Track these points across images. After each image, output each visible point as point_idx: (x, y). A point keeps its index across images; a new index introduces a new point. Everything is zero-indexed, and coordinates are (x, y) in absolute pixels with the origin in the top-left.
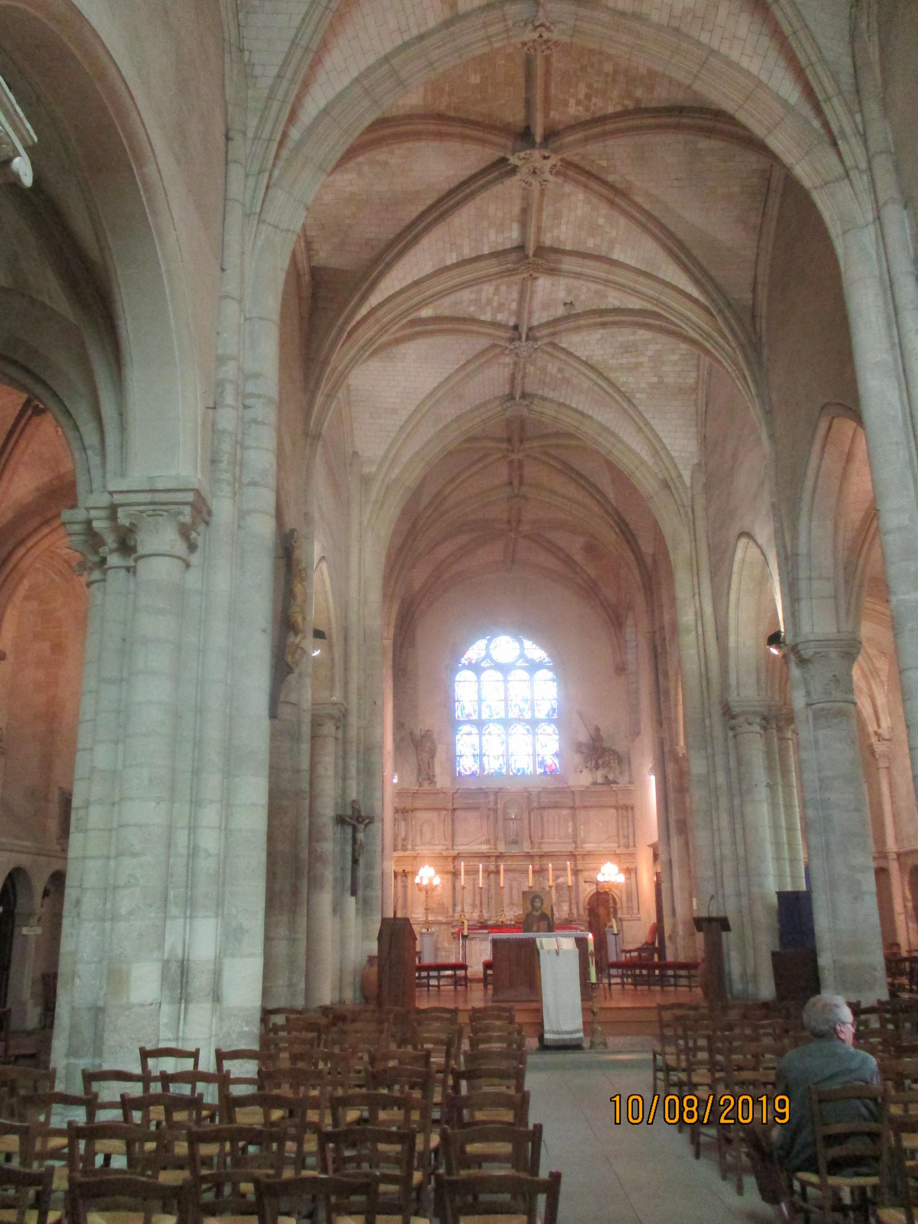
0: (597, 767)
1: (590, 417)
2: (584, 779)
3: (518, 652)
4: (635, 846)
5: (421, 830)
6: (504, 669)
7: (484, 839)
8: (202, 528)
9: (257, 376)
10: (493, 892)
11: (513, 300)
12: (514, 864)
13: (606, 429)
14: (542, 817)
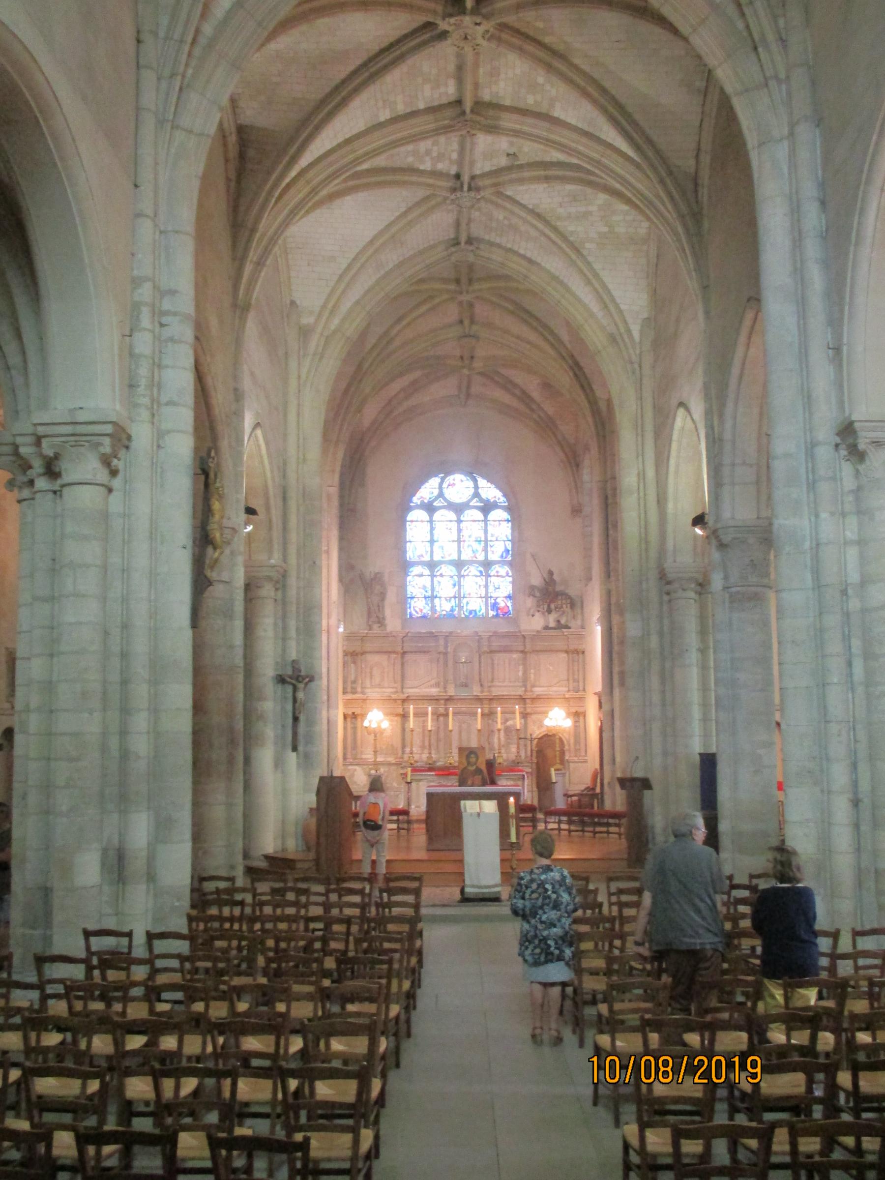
0: (549, 611)
1: (538, 265)
2: (537, 623)
3: (472, 490)
4: (584, 690)
5: (371, 673)
6: (459, 509)
7: (433, 682)
8: (122, 453)
9: (173, 292)
10: (442, 734)
11: (453, 151)
12: (463, 707)
13: (555, 278)
14: (493, 660)
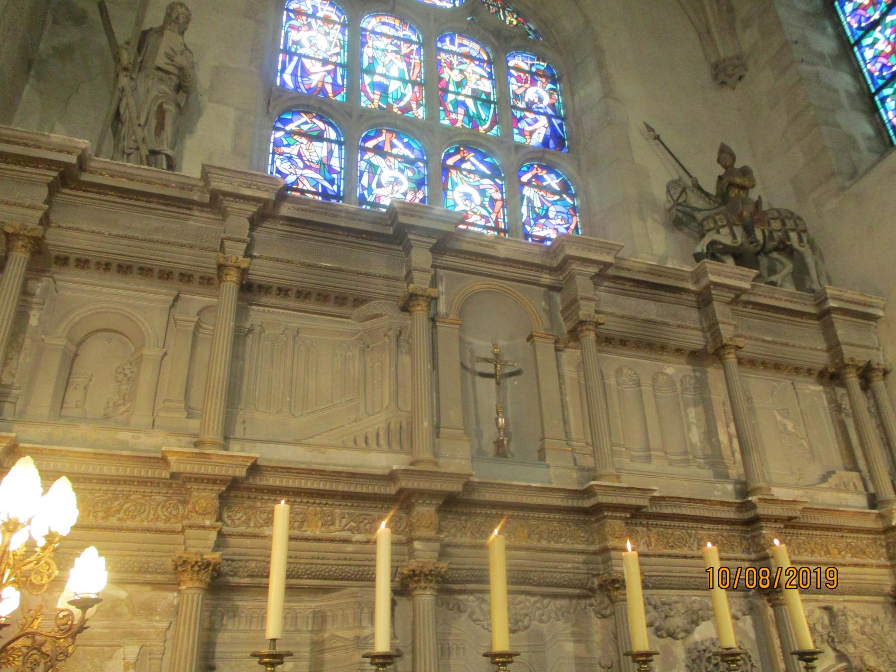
5: (71, 360)
7: (378, 422)
